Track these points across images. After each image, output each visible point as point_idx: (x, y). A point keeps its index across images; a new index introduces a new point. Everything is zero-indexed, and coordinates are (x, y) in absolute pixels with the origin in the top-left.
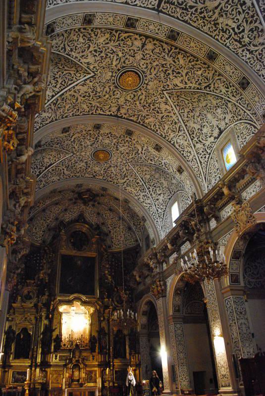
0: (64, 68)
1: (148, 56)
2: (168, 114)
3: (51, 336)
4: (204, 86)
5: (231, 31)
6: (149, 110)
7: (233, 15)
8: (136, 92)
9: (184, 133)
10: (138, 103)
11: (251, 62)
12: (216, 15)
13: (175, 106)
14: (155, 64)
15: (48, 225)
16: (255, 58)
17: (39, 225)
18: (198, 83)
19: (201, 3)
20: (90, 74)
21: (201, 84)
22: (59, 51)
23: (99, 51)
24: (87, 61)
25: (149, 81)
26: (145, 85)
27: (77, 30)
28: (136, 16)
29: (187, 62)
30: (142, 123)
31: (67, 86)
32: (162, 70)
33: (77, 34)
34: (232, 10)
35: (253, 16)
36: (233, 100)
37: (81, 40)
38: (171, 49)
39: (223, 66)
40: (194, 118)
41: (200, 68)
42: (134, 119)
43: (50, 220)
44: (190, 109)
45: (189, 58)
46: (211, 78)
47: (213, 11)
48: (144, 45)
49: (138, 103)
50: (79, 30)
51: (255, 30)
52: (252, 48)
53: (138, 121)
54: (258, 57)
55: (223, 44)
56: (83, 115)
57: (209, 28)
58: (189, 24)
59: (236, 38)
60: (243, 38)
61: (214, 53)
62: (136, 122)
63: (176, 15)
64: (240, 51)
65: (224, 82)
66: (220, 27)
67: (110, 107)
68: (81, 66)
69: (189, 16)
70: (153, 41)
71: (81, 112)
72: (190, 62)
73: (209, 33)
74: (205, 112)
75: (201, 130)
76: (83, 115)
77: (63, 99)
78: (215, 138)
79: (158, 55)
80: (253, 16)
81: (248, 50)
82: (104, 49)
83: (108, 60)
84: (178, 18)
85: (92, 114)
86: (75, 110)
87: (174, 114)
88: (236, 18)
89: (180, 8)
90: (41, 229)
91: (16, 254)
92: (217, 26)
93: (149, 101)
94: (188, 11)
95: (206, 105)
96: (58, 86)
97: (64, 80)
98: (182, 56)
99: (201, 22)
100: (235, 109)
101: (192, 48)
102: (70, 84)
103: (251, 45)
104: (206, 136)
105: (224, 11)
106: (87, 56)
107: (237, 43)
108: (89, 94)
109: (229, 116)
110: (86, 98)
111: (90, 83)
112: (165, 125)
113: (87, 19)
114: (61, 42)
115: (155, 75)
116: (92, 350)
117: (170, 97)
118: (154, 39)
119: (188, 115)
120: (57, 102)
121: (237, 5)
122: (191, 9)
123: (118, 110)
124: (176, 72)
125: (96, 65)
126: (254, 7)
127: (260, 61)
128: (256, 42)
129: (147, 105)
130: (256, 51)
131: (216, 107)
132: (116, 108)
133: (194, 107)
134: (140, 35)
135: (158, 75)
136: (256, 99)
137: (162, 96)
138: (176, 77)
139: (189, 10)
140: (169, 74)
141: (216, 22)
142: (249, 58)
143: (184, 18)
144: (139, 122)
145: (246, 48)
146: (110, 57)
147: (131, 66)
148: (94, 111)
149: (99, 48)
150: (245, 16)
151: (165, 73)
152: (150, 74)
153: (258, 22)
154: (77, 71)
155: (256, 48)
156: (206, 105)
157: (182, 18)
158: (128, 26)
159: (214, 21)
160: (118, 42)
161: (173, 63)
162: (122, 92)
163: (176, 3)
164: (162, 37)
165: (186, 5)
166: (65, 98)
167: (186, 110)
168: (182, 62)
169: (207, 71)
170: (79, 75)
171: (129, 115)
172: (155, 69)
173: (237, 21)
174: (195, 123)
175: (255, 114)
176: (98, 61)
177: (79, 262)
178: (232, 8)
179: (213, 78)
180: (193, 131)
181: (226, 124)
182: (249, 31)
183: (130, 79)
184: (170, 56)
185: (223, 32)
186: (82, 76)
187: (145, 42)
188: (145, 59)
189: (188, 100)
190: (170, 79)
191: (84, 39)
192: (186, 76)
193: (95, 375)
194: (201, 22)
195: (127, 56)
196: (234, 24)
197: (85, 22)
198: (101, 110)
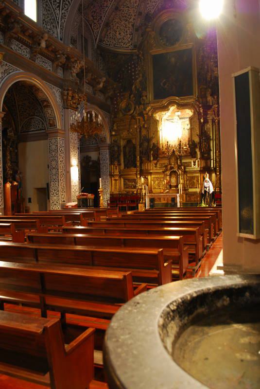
3: (148, 146)
15: (133, 26)
17: (122, 28)
43: (133, 17)
90: (127, 32)
91: (71, 69)
116: (193, 155)
177: (173, 60)
193: (198, 181)
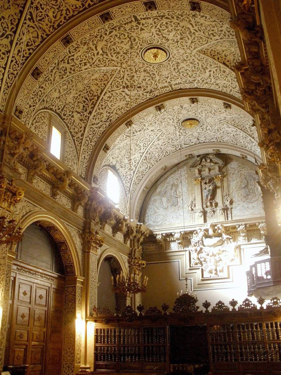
4: (33, 13)
5: (73, 54)
18: (39, 6)
21: (37, 10)
29: (68, 7)
34: (86, 57)
35: (74, 70)
39: (54, 50)
46: (40, 25)
47: (96, 44)
51: (65, 73)
65: (35, 42)
69: (107, 28)
72: (67, 9)
89: (118, 26)
98: (77, 6)
99: (95, 34)
103: (57, 70)
107: (62, 58)
121: (88, 60)
128: (58, 74)
130: (51, 75)
139: (111, 30)
155: (53, 75)
159: (89, 43)
165: (116, 30)
169: (49, 24)
175: (8, 87)
179: (40, 28)
194: (95, 34)
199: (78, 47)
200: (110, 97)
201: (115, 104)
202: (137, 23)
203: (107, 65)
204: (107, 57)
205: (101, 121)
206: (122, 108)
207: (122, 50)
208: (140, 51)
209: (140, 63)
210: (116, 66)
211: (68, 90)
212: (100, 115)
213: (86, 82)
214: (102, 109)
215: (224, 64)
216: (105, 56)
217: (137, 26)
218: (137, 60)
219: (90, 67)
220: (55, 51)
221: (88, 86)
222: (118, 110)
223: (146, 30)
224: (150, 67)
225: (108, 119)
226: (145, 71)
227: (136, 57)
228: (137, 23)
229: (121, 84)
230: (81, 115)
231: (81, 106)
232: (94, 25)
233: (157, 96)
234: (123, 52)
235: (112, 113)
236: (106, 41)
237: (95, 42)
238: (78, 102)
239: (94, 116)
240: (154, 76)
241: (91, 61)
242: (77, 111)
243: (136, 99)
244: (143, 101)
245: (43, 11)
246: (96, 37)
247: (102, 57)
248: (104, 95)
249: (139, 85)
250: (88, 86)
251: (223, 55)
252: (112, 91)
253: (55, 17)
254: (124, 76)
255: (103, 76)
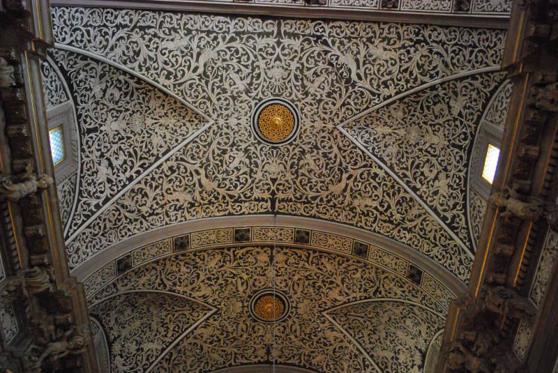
0: (173, 308)
1: (283, 270)
2: (341, 344)
5: (375, 212)
6: (312, 344)
7: (369, 192)
8: (284, 321)
9: (373, 369)
10: (292, 337)
11: (416, 243)
12: (348, 199)
13: (346, 330)
14: (296, 278)
16: (418, 237)
18: (362, 290)
19: (324, 190)
20: (211, 310)
22: (156, 289)
23: (214, 279)
24: (201, 294)
25: (297, 303)
26: (294, 309)
27: (173, 259)
28: (246, 226)
30: (308, 366)
31: (183, 332)
32: (309, 284)
33: (175, 264)
34: (366, 187)
35: (393, 187)
36: (416, 301)
37: (184, 269)
38: (309, 254)
39: (380, 259)
40: (380, 342)
41: (356, 269)
42: (295, 361)
44: (371, 330)
45: (337, 259)
46: (376, 279)
48: (271, 258)
49: (292, 337)
50: (176, 257)
51: (403, 201)
52: (409, 225)
53: (302, 364)
54: (421, 233)
55: (370, 230)
56: (216, 370)
57: (346, 216)
58: (319, 218)
59: (383, 218)
60: (392, 216)
61: (361, 245)
62: (299, 366)
63: (298, 213)
64: (395, 233)
65: (394, 279)
66: (358, 210)
67: (255, 351)
68: (195, 302)
69: (315, 208)
70: (282, 249)
71: (212, 366)
72: (339, 264)
73: (348, 222)
74: (393, 330)
75: (397, 359)
76: (216, 370)
77: (181, 350)
78: (420, 367)
79: (296, 266)
80: (393, 187)
81: (405, 229)
82: (220, 274)
83: (230, 286)
84: (302, 215)
85: (230, 365)
86: (203, 364)
87: (350, 342)
88: (373, 195)
89: (301, 203)
92: (354, 210)
93: (308, 331)
94: (312, 204)
95: (390, 319)
96: (169, 335)
97: (178, 325)
99: (332, 211)
100: (425, 315)
101: (332, 245)
102: (187, 329)
103: (406, 221)
104: (406, 367)
105: (356, 191)
106: (200, 288)
107: (387, 224)
108: (217, 337)
109: (423, 328)
110: (215, 343)
111: (215, 322)
112: (341, 361)
113: (179, 243)
114: (154, 277)
115: (302, 292)
117: (334, 318)
118: (282, 247)
119: (371, 340)
120: (171, 356)
122: (314, 200)
123: (268, 353)
124: (327, 282)
125: (216, 297)
126: (389, 175)
127: (426, 238)
128: (410, 216)
129: (307, 337)
130: (415, 227)
131: (402, 318)
132: (264, 351)
133: (375, 324)
134: (263, 247)
135: (305, 292)
136: (438, 292)
137: (322, 319)
138: (329, 288)
139: (313, 202)
140: (320, 287)
141: (351, 207)
142: (411, 239)
143: (311, 213)
144: (304, 364)
145: (402, 227)
146: (232, 283)
147: (266, 288)
148: (232, 361)
149: (213, 275)
150: (383, 189)
151: (314, 287)
152: (296, 293)
153: (402, 191)
154: (194, 310)
155: (414, 223)
156: (390, 319)
157: (308, 213)
158: (239, 240)
160: (236, 262)
161: (319, 271)
162: (264, 326)
163: (293, 199)
164: (288, 242)
165: (307, 198)
166: (183, 350)
167: (366, 332)
168: (329, 267)
169: (367, 271)
170: (197, 314)
171: (286, 357)
172: (298, 284)
173: (377, 198)
174: (384, 349)
176: (216, 291)
178: (364, 185)
179: (378, 278)
180: (386, 363)
181: (426, 341)
182: (397, 205)
183: (270, 306)
184: (312, 263)
185: (365, 216)
186: (201, 315)
187: (272, 253)
188: (280, 276)
189: (362, 317)
190: (324, 293)
191: (187, 268)
192: (343, 284)
194: (332, 211)
195: (255, 277)
196: (374, 202)
197: (177, 247)
198: (242, 357)
199: (363, 213)
200: (385, 83)
201: (387, 61)
202: (276, 194)
203: (352, 146)
204: (342, 159)
205: (431, 51)
206: (384, 40)
207: (318, 156)
208: (295, 140)
209: (305, 115)
210: (341, 133)
211: (430, 157)
212: (423, 65)
213: (402, 132)
214: (411, 74)
215: (166, 95)
216: (344, 165)
217: (278, 190)
218: (308, 123)
219: (374, 164)
220: (380, 257)
221: (405, 122)
222: (392, 42)
223: (269, 177)
224: (295, 99)
225: (418, 42)
226: (306, 94)
227: (306, 130)
228: (276, 194)
229: (354, 94)
230: (450, 98)
231: (437, 108)
232: (321, 238)
233: (313, 20)
234: (318, 153)
235: (404, 47)
236: (328, 190)
237: (341, 199)
238: (436, 117)
239: (432, 77)
240: (298, 73)
241: (365, 175)
242: (450, 112)
243: (349, 39)
244: (343, 24)
245: (363, 283)
246: (334, 206)
247: (349, 166)
248: (390, 97)
249: (330, 69)
250: (405, 122)
251: (167, 107)
252: (373, 94)
253: (356, 269)
254: (341, 107)
255: (371, 124)
